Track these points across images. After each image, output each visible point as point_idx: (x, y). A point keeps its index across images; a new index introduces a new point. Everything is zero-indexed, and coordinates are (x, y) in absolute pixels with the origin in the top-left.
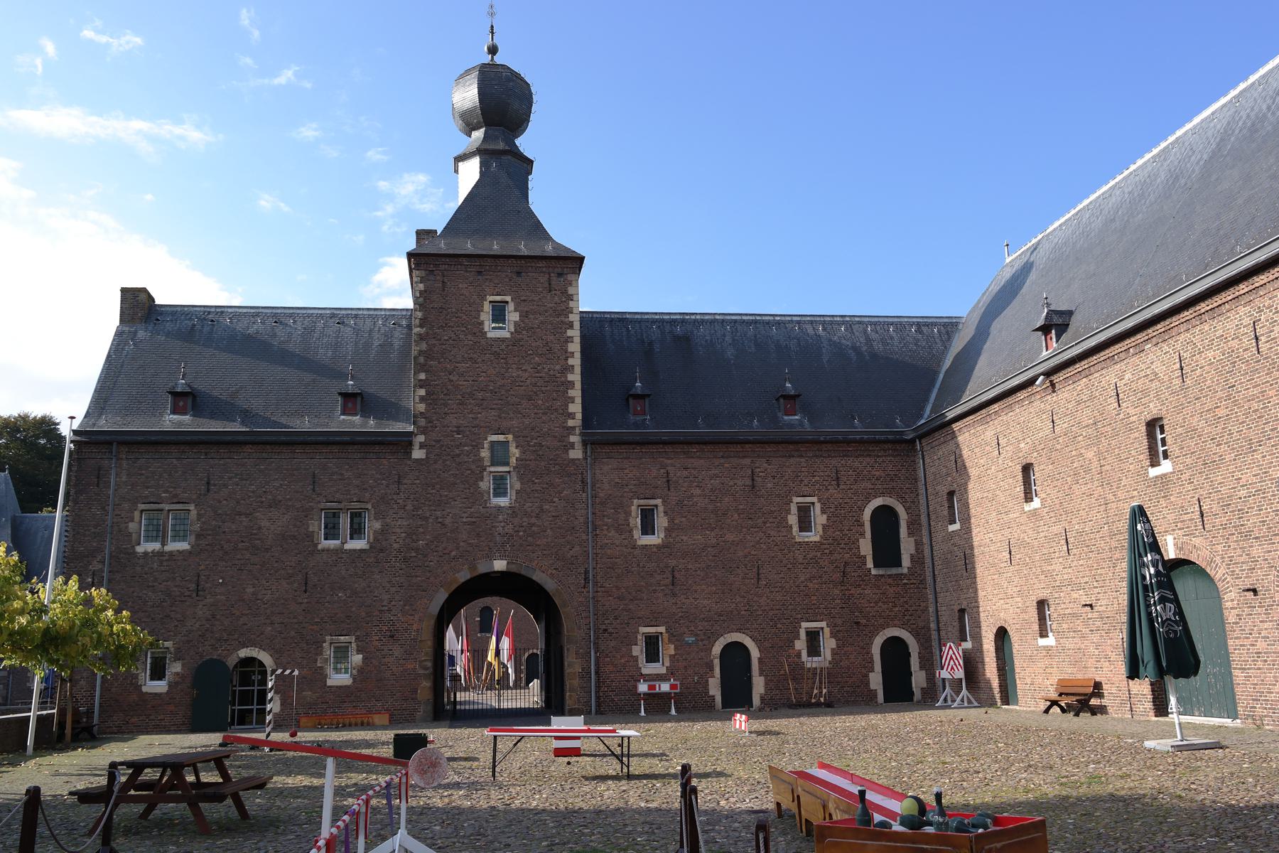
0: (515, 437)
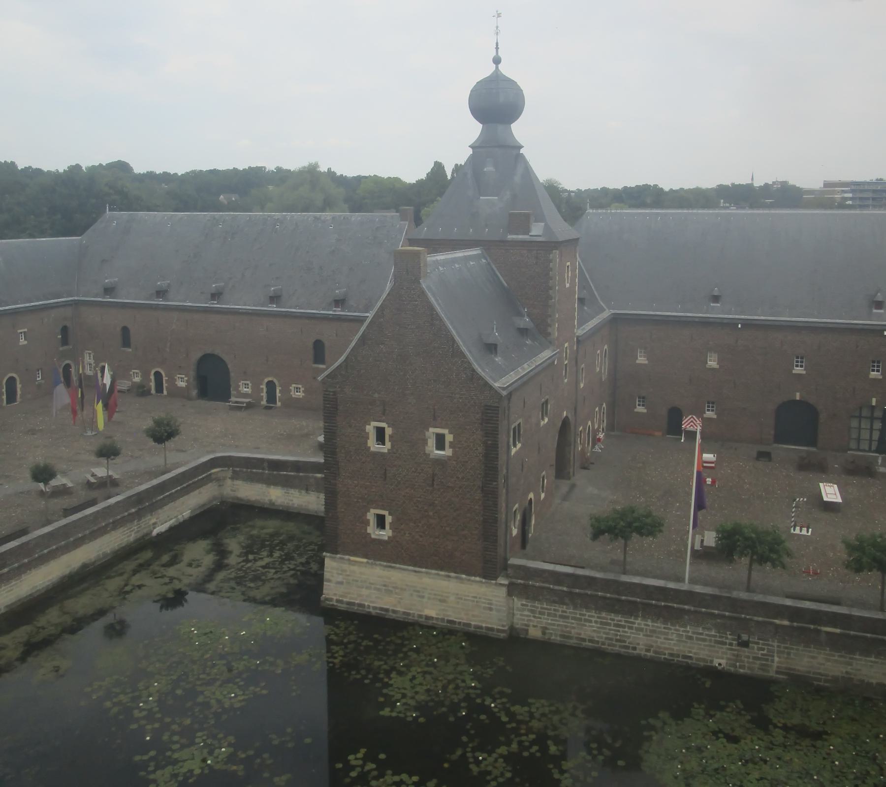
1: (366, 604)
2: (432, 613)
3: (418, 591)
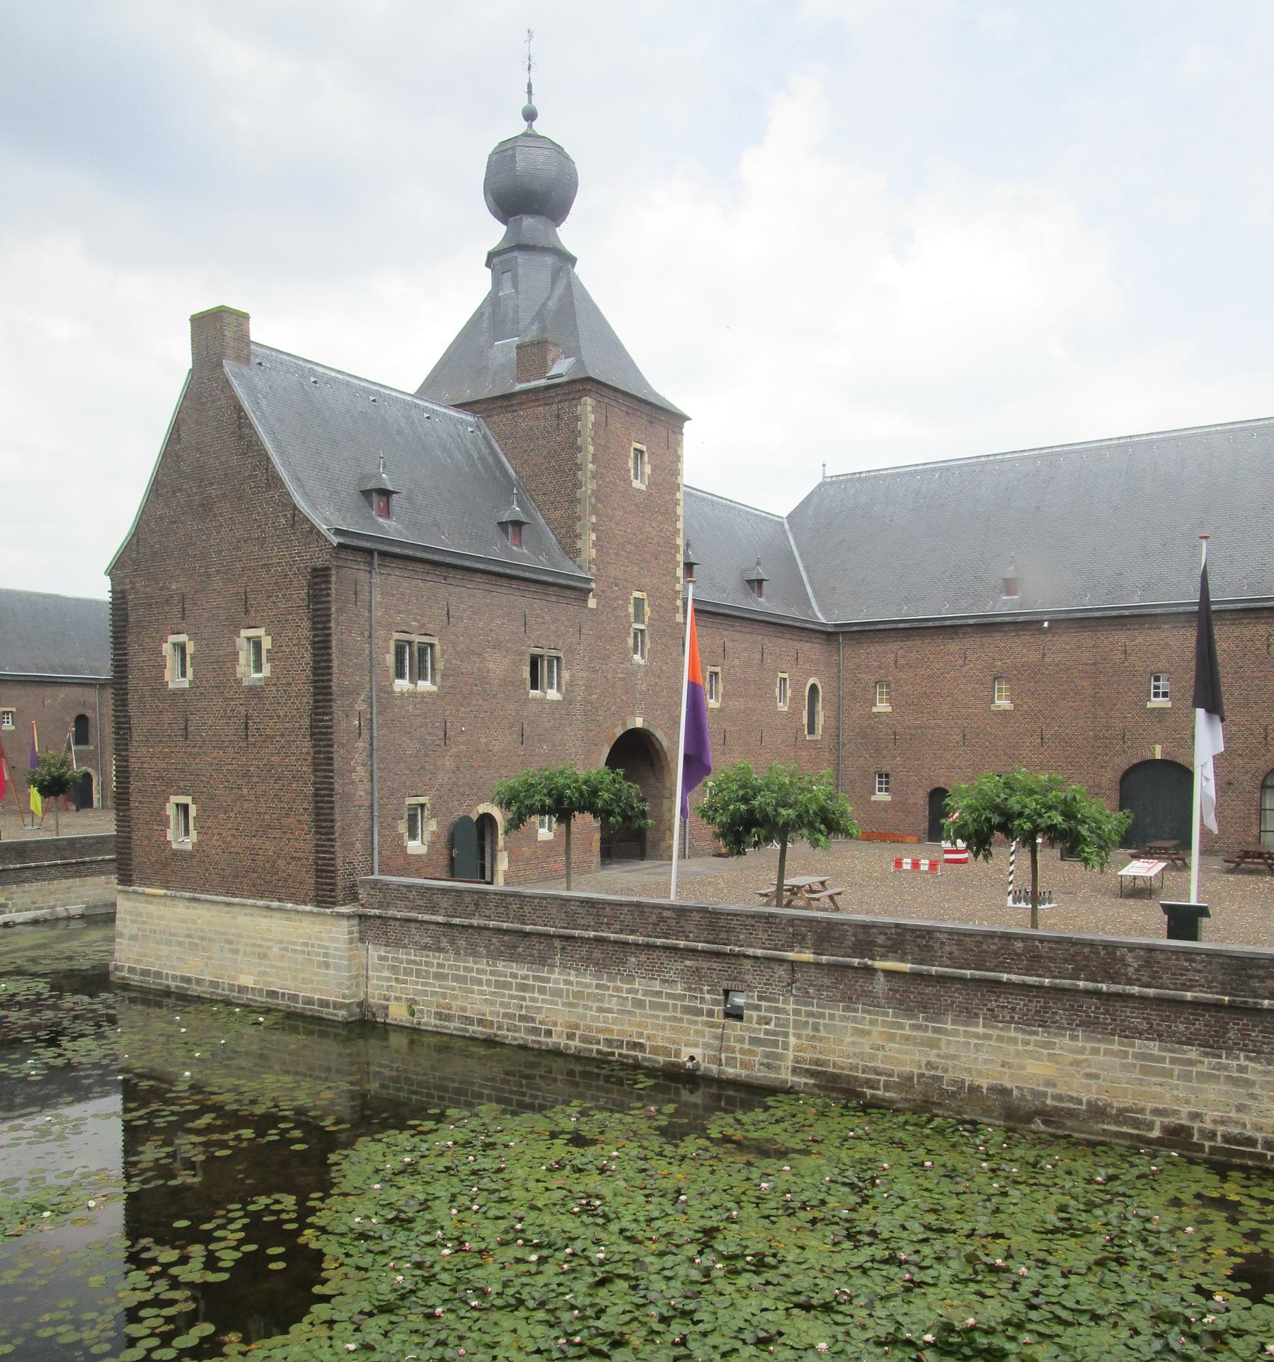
0: (648, 595)
1: (165, 972)
2: (247, 980)
3: (230, 942)
